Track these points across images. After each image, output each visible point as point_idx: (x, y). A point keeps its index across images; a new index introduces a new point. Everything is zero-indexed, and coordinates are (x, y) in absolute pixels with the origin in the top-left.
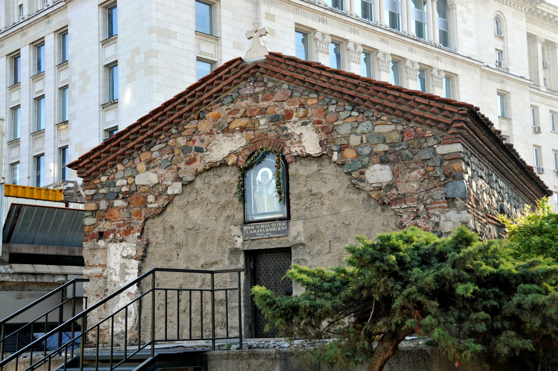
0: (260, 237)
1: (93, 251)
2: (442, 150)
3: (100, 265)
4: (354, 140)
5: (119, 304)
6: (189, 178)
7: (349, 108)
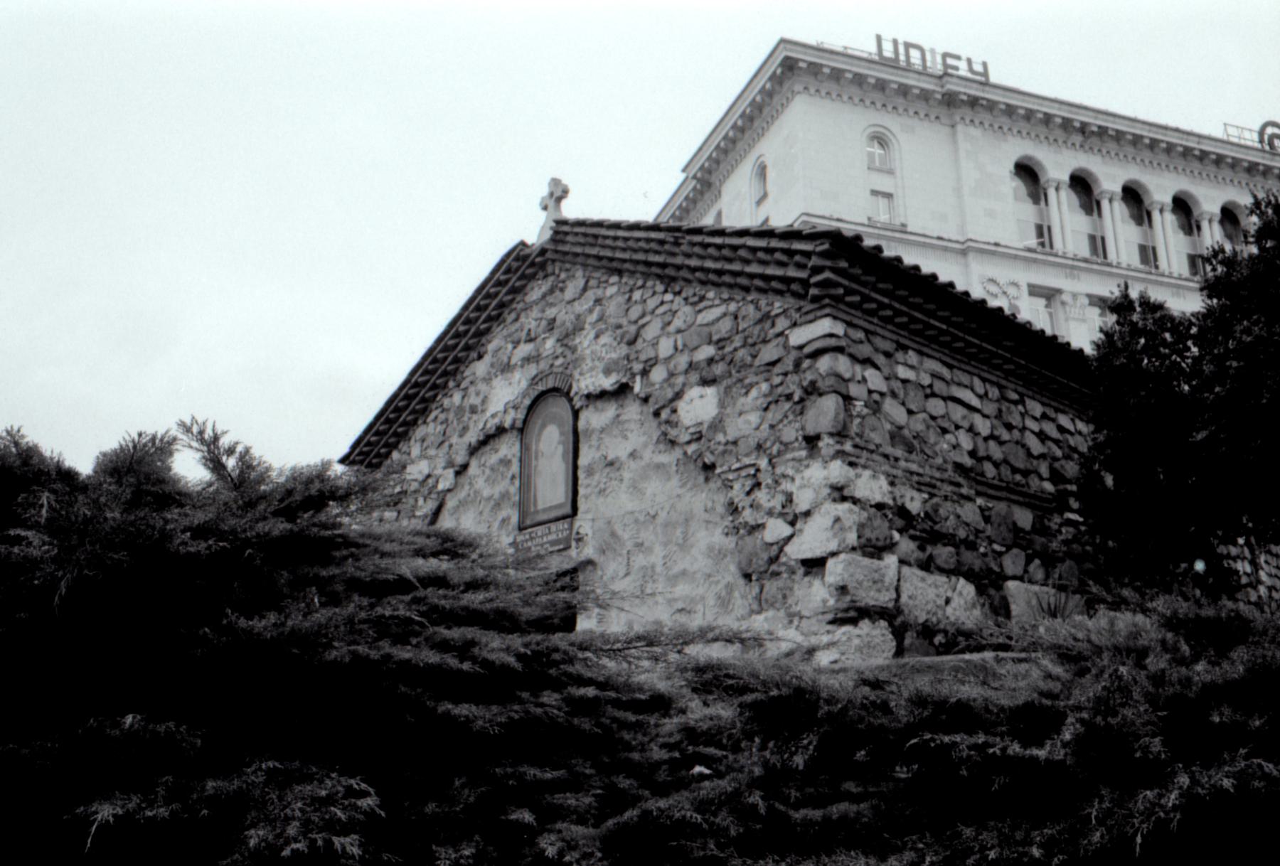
2: (798, 336)
6: (460, 459)
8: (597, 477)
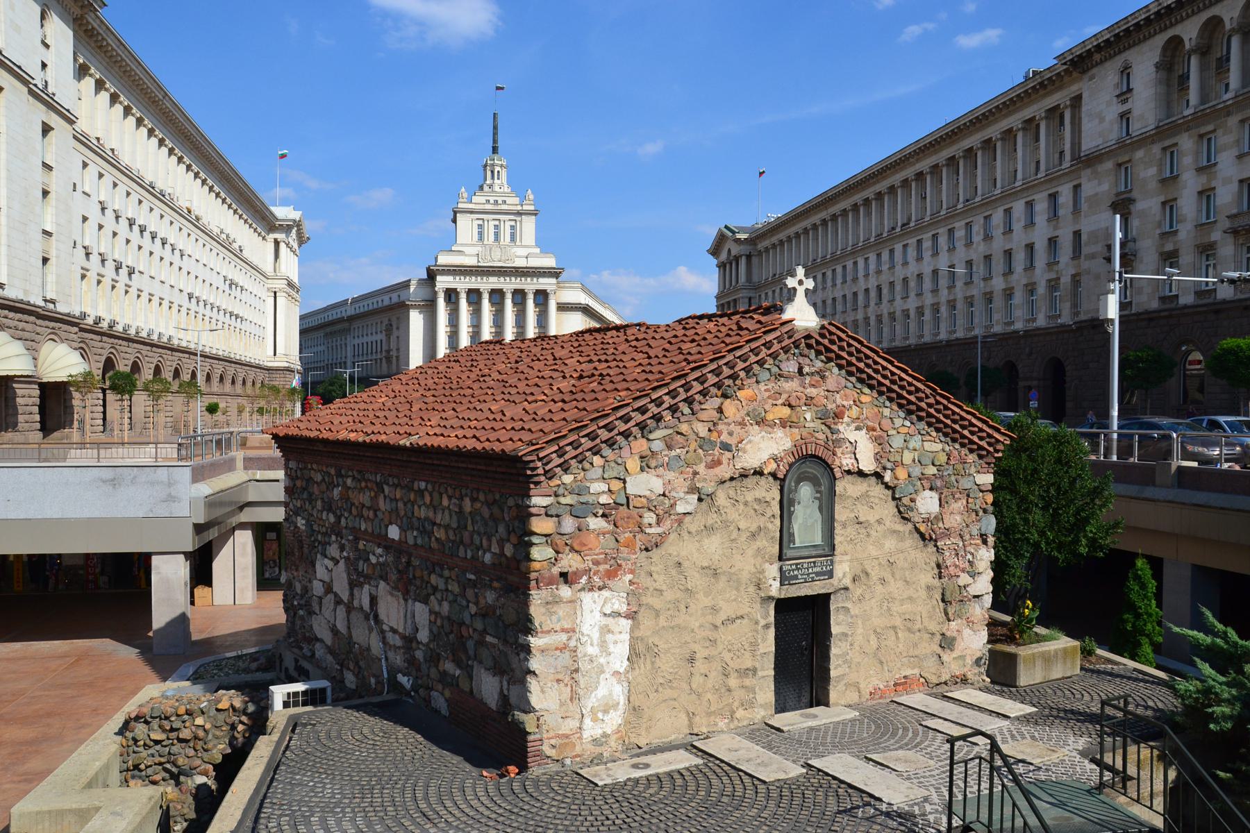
1: (549, 606)
3: (563, 630)
4: (908, 457)
5: (597, 692)
7: (902, 415)
8: (849, 529)
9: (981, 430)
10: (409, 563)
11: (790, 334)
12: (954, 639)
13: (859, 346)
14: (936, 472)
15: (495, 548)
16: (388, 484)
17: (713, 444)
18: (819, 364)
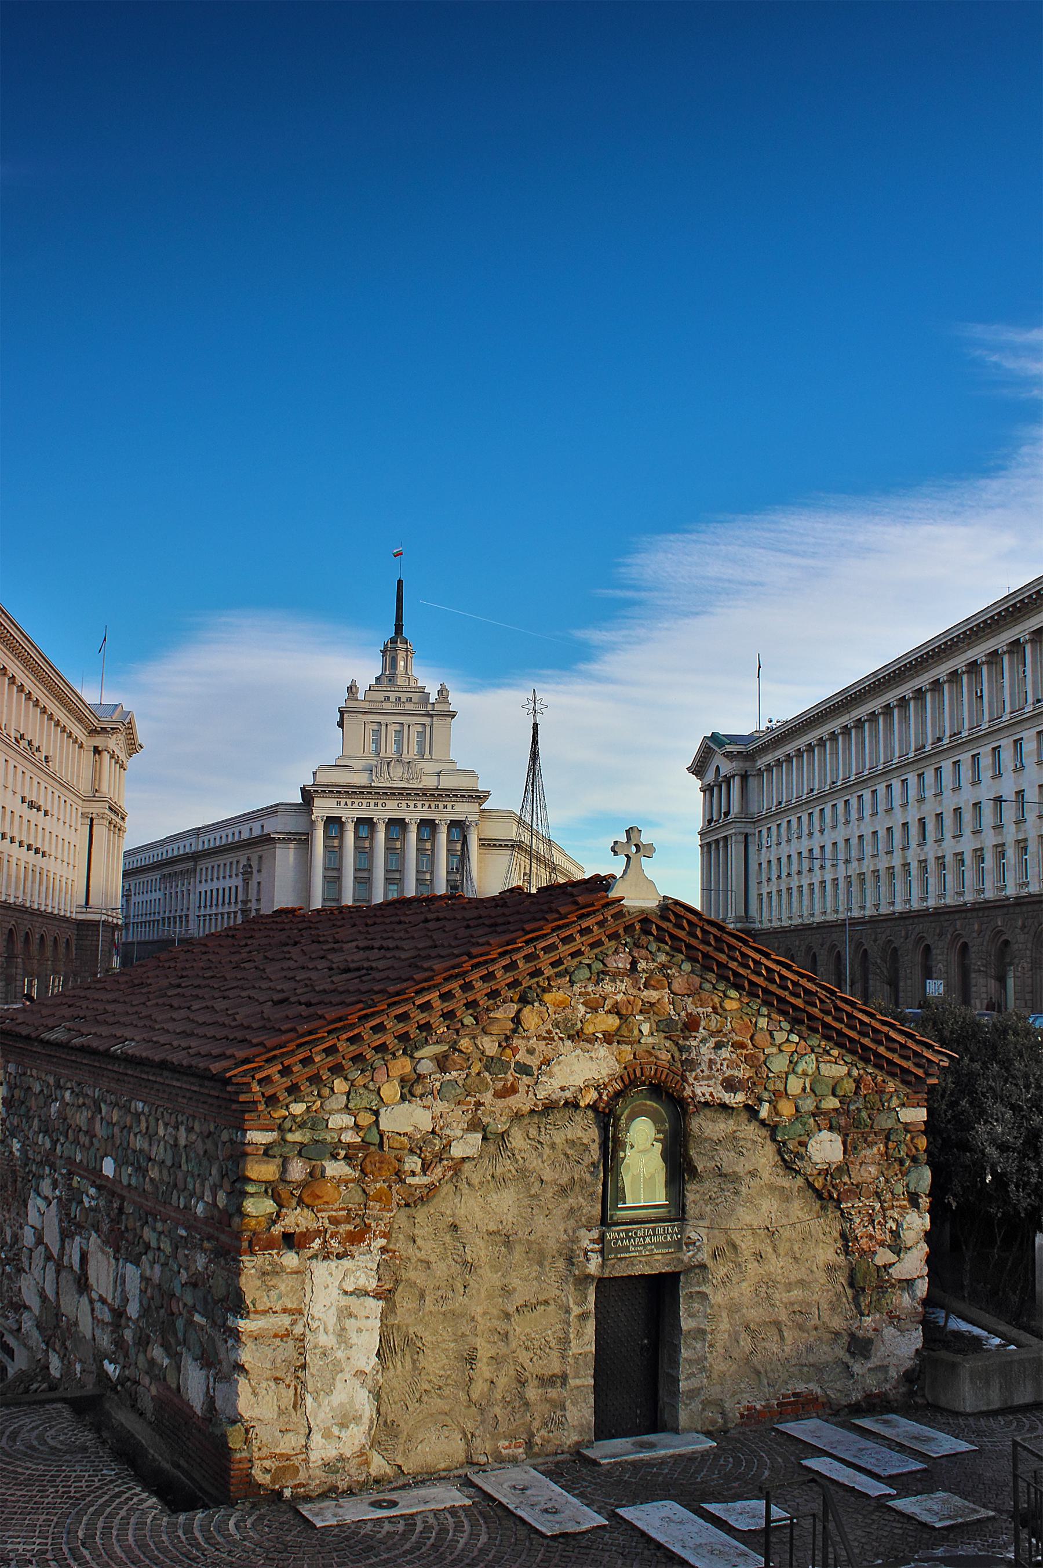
0: (635, 1254)
3: (285, 1311)
4: (794, 1085)
5: (332, 1397)
7: (786, 1026)
9: (903, 1046)
10: (121, 1210)
11: (619, 915)
12: (870, 1341)
13: (718, 933)
14: (838, 1105)
15: (208, 1198)
16: (105, 1102)
17: (505, 1066)
18: (662, 958)
